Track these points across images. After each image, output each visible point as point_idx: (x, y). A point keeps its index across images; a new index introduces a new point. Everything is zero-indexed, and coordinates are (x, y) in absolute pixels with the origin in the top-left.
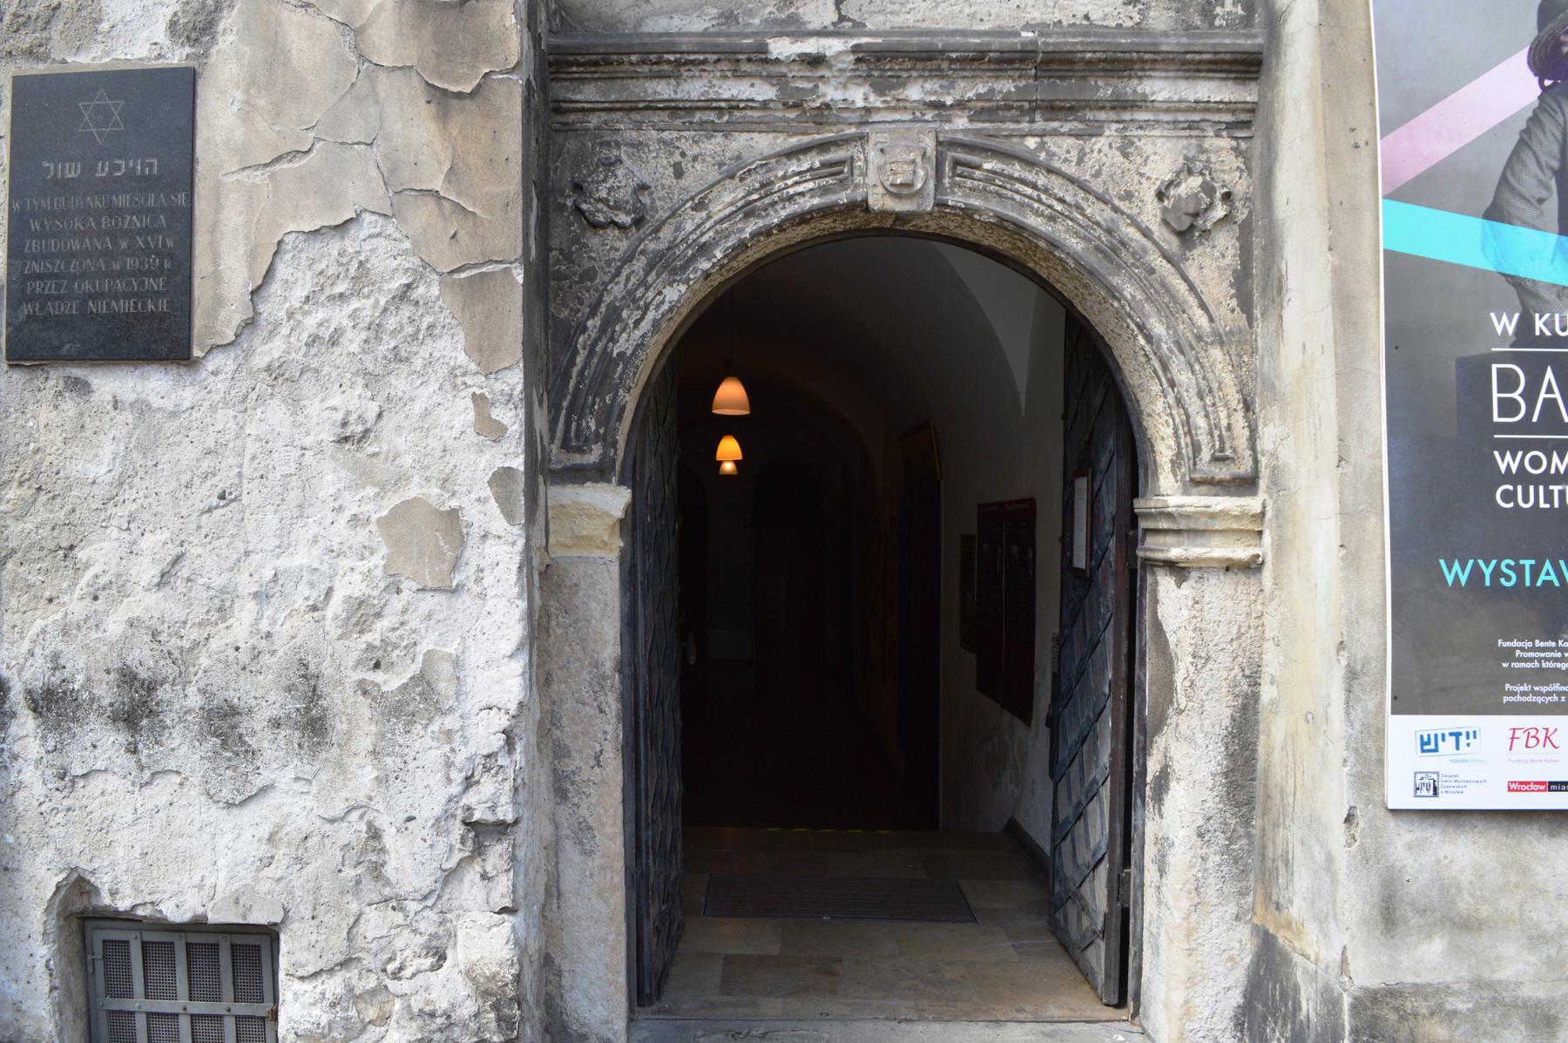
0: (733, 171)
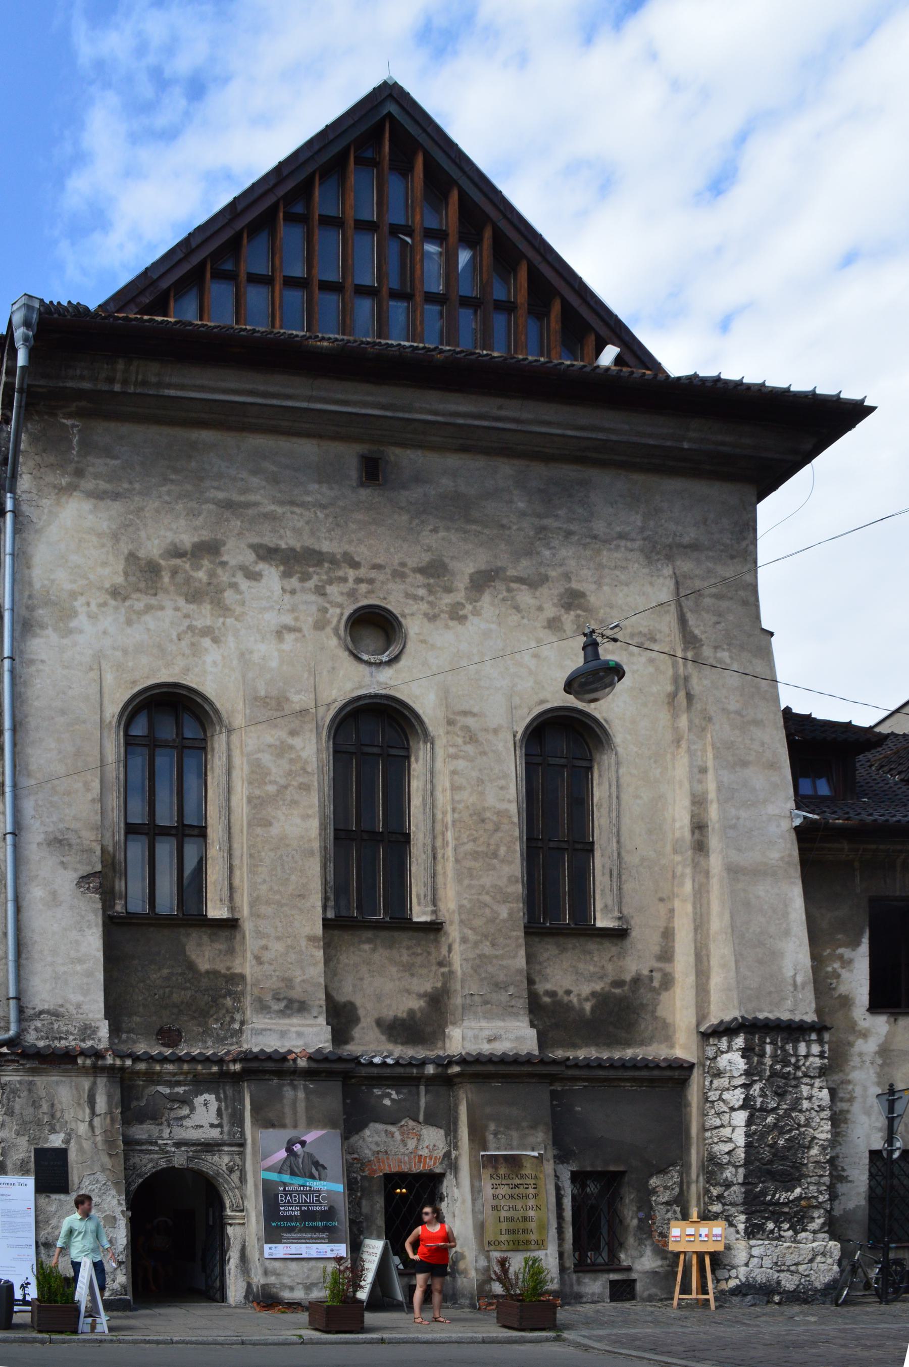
0: (151, 1161)
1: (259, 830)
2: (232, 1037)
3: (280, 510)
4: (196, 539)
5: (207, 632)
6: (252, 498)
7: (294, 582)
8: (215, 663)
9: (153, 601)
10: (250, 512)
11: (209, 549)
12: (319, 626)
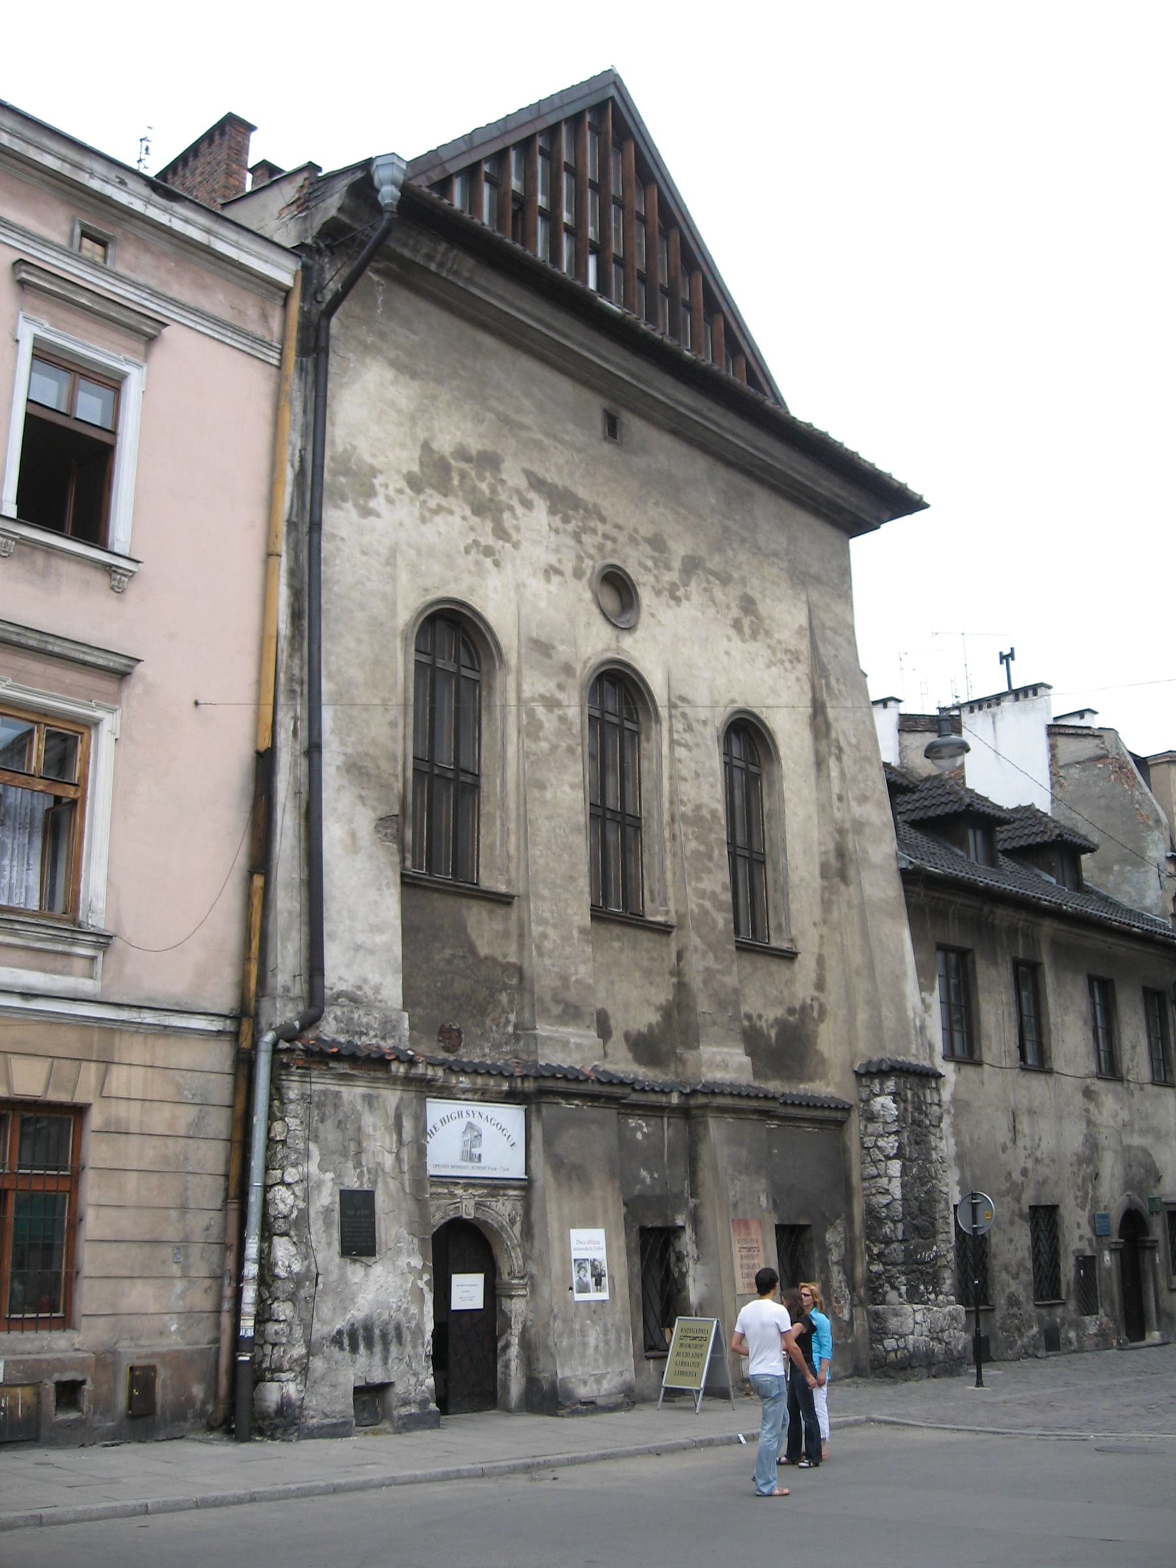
0: (438, 1208)
1: (536, 793)
2: (506, 1044)
3: (547, 442)
4: (480, 447)
5: (488, 551)
6: (527, 420)
7: (557, 521)
8: (495, 589)
9: (444, 502)
10: (523, 434)
11: (489, 461)
12: (578, 574)
